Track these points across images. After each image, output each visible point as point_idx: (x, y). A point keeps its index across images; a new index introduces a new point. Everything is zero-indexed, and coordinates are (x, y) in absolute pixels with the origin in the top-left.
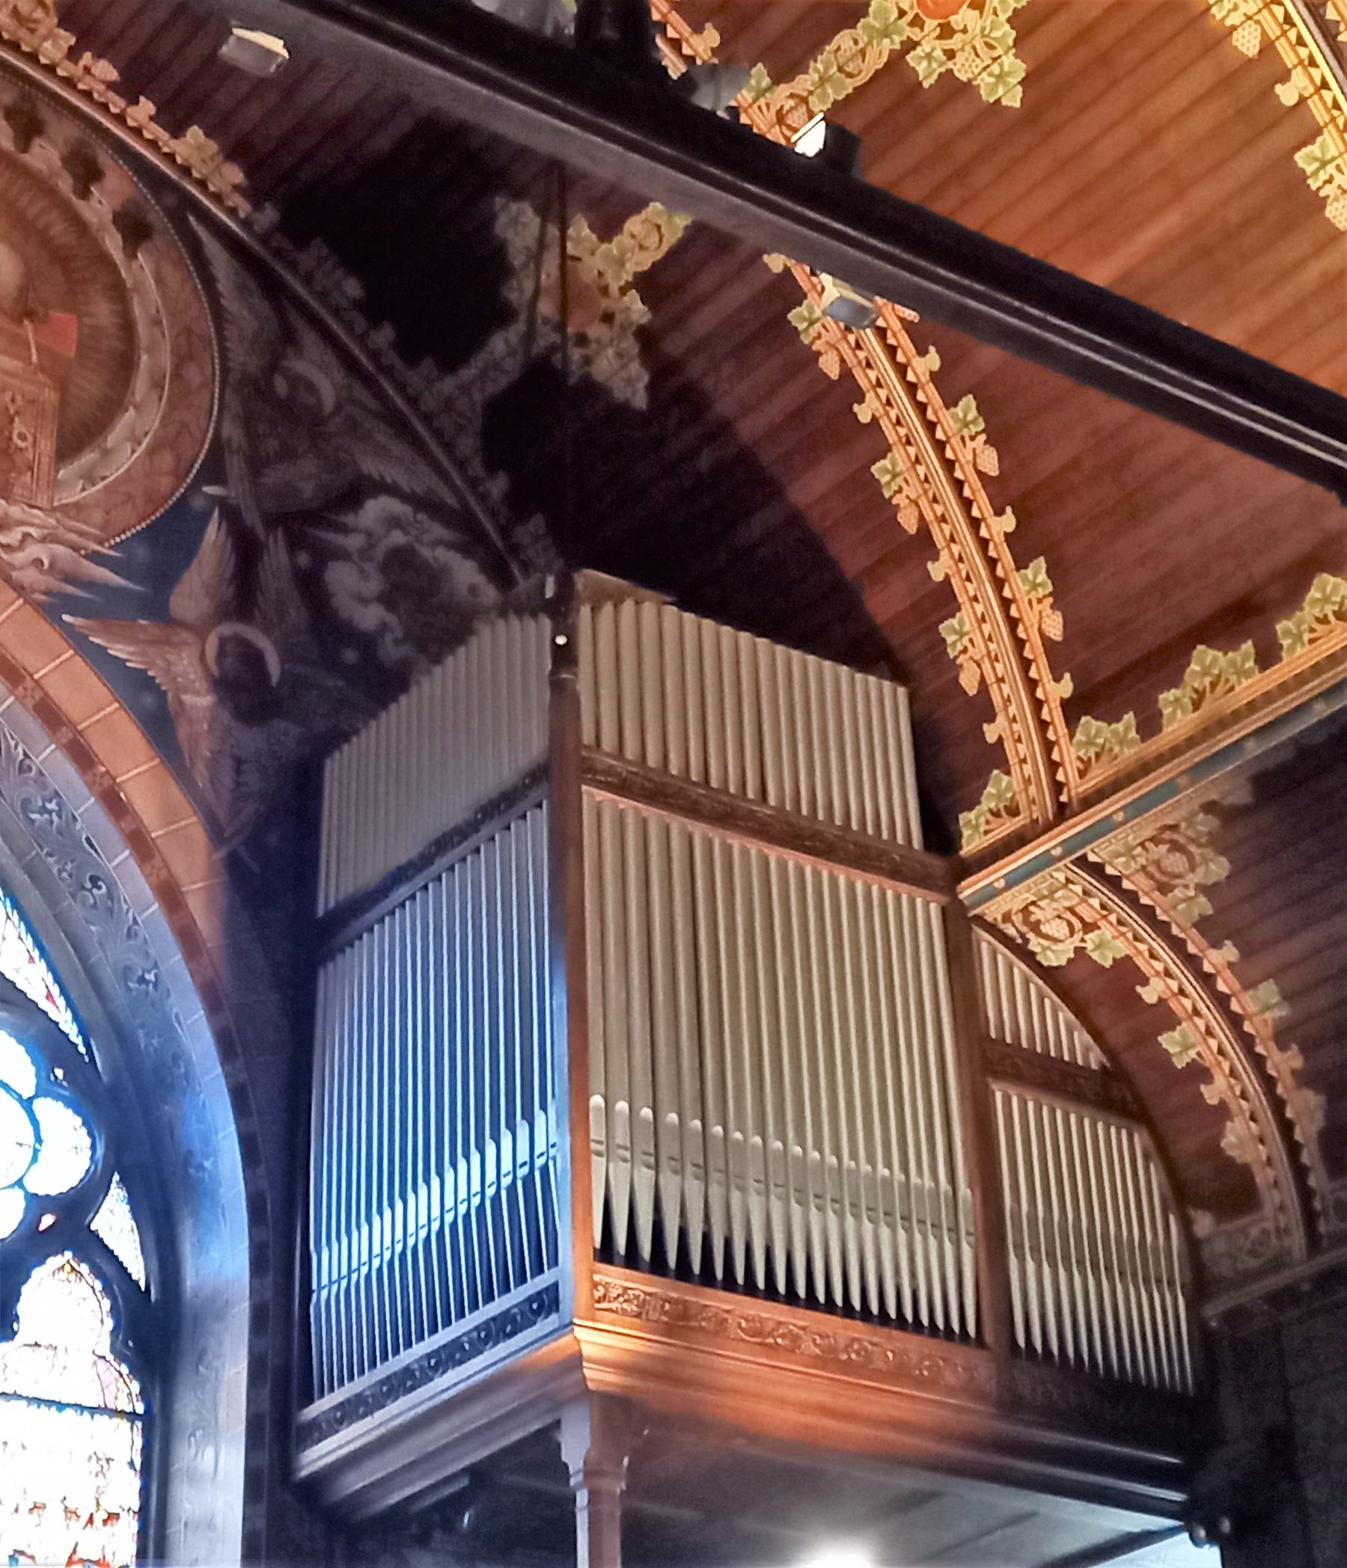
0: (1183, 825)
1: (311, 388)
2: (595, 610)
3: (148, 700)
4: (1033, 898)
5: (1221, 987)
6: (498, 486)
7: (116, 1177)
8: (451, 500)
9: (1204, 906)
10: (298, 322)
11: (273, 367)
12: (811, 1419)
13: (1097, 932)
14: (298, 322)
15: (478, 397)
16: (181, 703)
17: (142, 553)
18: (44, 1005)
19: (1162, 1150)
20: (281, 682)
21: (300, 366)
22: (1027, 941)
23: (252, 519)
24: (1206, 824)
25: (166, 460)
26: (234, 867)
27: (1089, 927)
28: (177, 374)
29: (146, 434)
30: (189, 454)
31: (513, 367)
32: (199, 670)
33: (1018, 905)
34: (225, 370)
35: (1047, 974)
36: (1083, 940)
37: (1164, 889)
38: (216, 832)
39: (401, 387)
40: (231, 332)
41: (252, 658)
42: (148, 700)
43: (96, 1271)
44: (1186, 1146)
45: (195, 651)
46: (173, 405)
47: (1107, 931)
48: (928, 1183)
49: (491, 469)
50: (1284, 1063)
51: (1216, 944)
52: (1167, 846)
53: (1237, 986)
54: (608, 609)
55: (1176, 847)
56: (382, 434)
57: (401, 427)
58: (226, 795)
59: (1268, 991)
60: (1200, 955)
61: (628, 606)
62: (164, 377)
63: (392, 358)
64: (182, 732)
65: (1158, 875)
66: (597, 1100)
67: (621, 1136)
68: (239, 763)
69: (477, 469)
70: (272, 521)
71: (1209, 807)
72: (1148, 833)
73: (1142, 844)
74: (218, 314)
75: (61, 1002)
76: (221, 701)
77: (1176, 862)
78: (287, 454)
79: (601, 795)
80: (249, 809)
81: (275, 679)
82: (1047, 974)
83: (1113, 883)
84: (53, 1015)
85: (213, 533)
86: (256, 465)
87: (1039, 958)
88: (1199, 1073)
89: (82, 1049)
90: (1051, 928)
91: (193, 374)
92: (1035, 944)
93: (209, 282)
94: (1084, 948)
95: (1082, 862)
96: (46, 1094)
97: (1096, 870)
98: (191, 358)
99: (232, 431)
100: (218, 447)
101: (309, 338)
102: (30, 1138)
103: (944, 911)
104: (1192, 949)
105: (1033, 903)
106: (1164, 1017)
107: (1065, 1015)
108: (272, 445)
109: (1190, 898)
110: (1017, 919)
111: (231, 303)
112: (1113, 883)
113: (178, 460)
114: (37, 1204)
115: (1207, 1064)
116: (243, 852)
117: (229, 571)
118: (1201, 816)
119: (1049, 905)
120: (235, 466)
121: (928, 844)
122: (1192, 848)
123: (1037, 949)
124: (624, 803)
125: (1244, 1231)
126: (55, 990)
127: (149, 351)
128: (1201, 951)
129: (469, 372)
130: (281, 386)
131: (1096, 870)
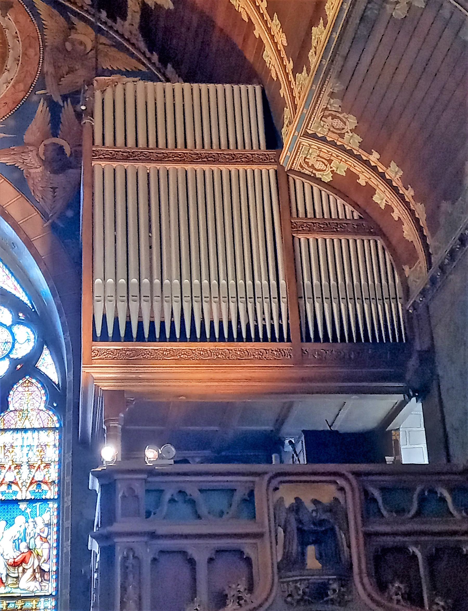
0: (329, 106)
1: (81, 43)
2: (103, 92)
3: (16, 175)
4: (304, 156)
5: (380, 170)
6: (155, 57)
7: (45, 347)
8: (144, 69)
9: (357, 139)
10: (74, 19)
11: (66, 39)
12: (285, 384)
13: (333, 162)
14: (74, 19)
15: (136, 26)
16: (30, 173)
17: (12, 123)
18: (14, 292)
19: (389, 246)
20: (71, 155)
21: (74, 36)
22: (315, 174)
23: (57, 99)
24: (336, 104)
25: (21, 86)
26: (53, 227)
27: (330, 161)
28: (25, 54)
29: (12, 79)
30: (30, 82)
31: (137, 8)
32: (37, 159)
33: (301, 161)
34: (45, 46)
35: (328, 185)
36: (331, 168)
37: (342, 136)
38: (44, 216)
39: (117, 32)
40: (46, 32)
41: (61, 149)
42: (16, 175)
43: (39, 381)
44: (394, 241)
45: (35, 152)
46: (23, 66)
47: (335, 162)
48: (265, 282)
49: (151, 51)
50: (409, 194)
51: (371, 153)
52: (330, 117)
53: (385, 168)
54: (109, 91)
55: (334, 117)
56: (113, 52)
57: (119, 47)
58: (49, 202)
59: (393, 165)
60: (368, 159)
61: (119, 88)
62: (19, 56)
63: (110, 22)
64: (30, 182)
65: (339, 132)
66: (98, 281)
67: (110, 291)
68: (54, 189)
69: (148, 54)
70: (65, 98)
71: (332, 95)
72: (320, 114)
73: (321, 120)
74: (42, 27)
75: (21, 290)
76: (46, 168)
77: (337, 123)
78: (71, 71)
79: (103, 163)
80: (59, 205)
81: (68, 155)
82: (328, 185)
83: (323, 140)
84: (17, 295)
85: (42, 108)
86: (59, 78)
87: (323, 180)
88: (389, 208)
89: (30, 305)
90: (319, 165)
91: (31, 52)
92: (318, 174)
93: (36, 15)
94: (334, 170)
95: (306, 135)
96: (19, 323)
97: (314, 136)
98: (30, 46)
99: (48, 68)
100: (43, 75)
101: (80, 25)
102: (11, 341)
103: (276, 171)
104: (365, 158)
105: (305, 158)
106: (371, 191)
107: (340, 202)
108: (65, 69)
109: (352, 136)
110: (305, 166)
111: (47, 22)
112: (323, 140)
113: (25, 85)
114: (15, 362)
115: (390, 204)
116: (57, 222)
117: (49, 119)
118: (332, 101)
119: (310, 156)
120: (49, 80)
121: (269, 146)
122: (338, 115)
123: (320, 176)
124: (115, 164)
125: (416, 269)
126: (18, 286)
127: (13, 49)
128: (367, 157)
129: (129, 17)
130: (68, 46)
131: (314, 136)
